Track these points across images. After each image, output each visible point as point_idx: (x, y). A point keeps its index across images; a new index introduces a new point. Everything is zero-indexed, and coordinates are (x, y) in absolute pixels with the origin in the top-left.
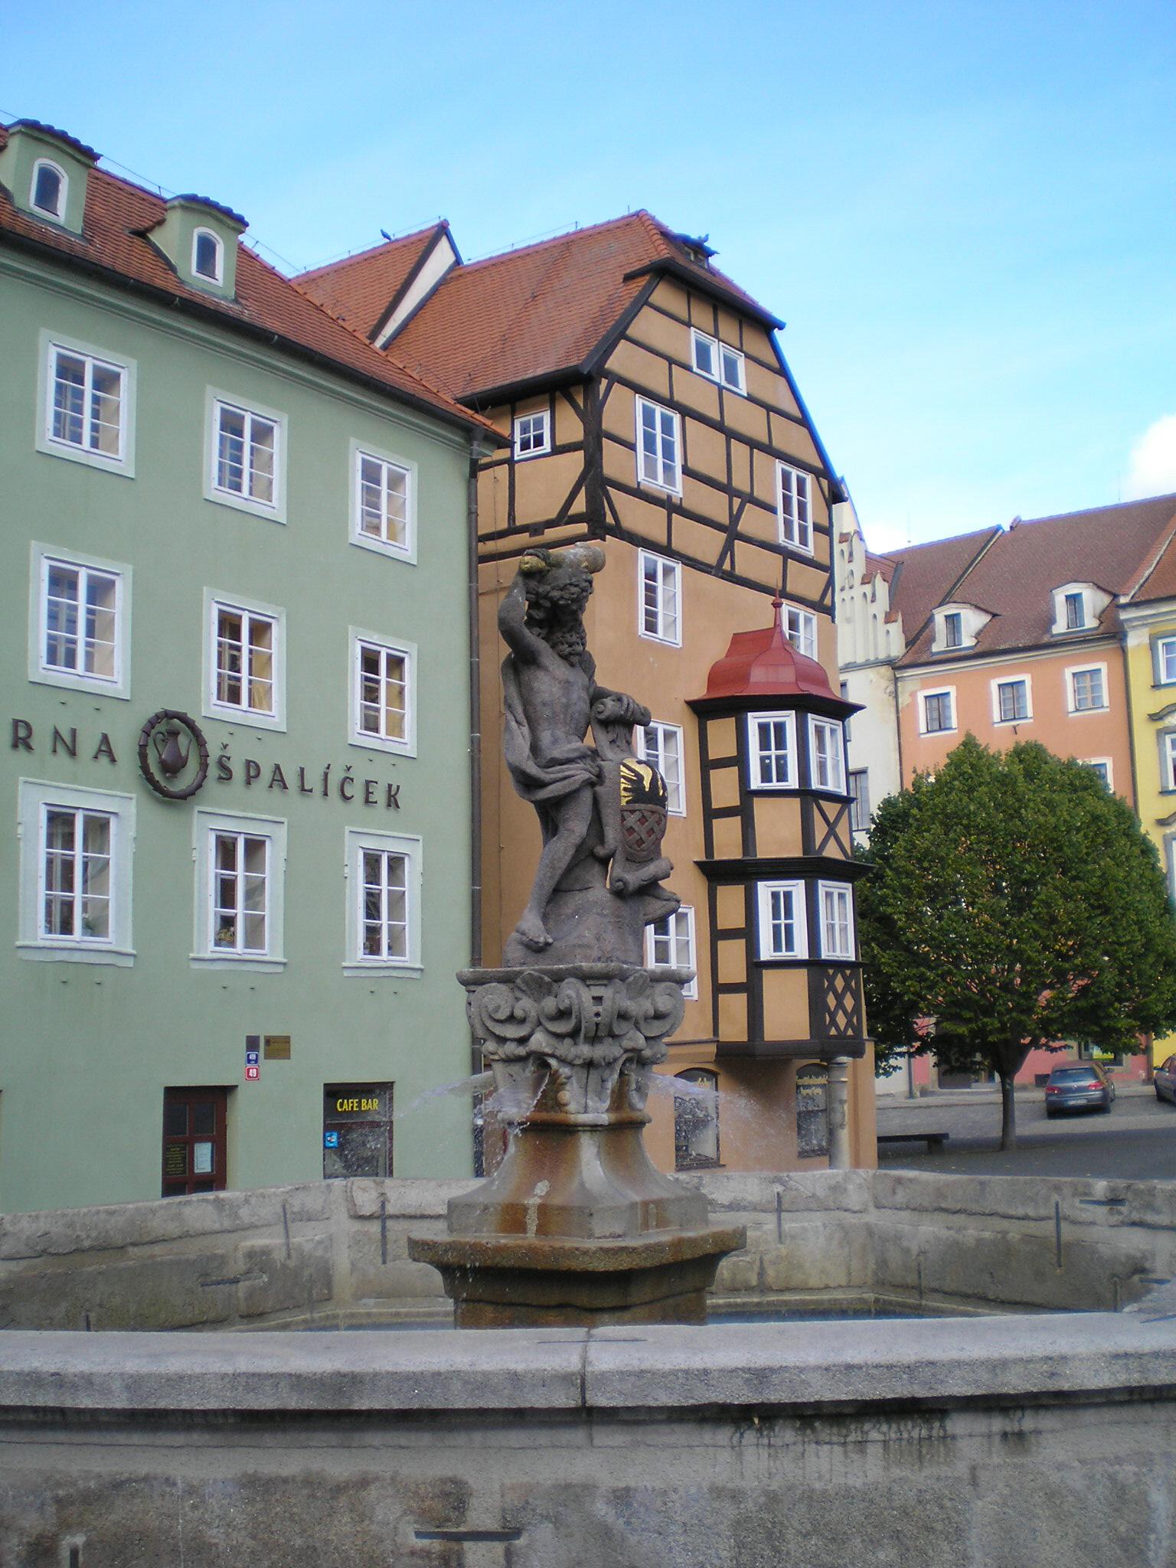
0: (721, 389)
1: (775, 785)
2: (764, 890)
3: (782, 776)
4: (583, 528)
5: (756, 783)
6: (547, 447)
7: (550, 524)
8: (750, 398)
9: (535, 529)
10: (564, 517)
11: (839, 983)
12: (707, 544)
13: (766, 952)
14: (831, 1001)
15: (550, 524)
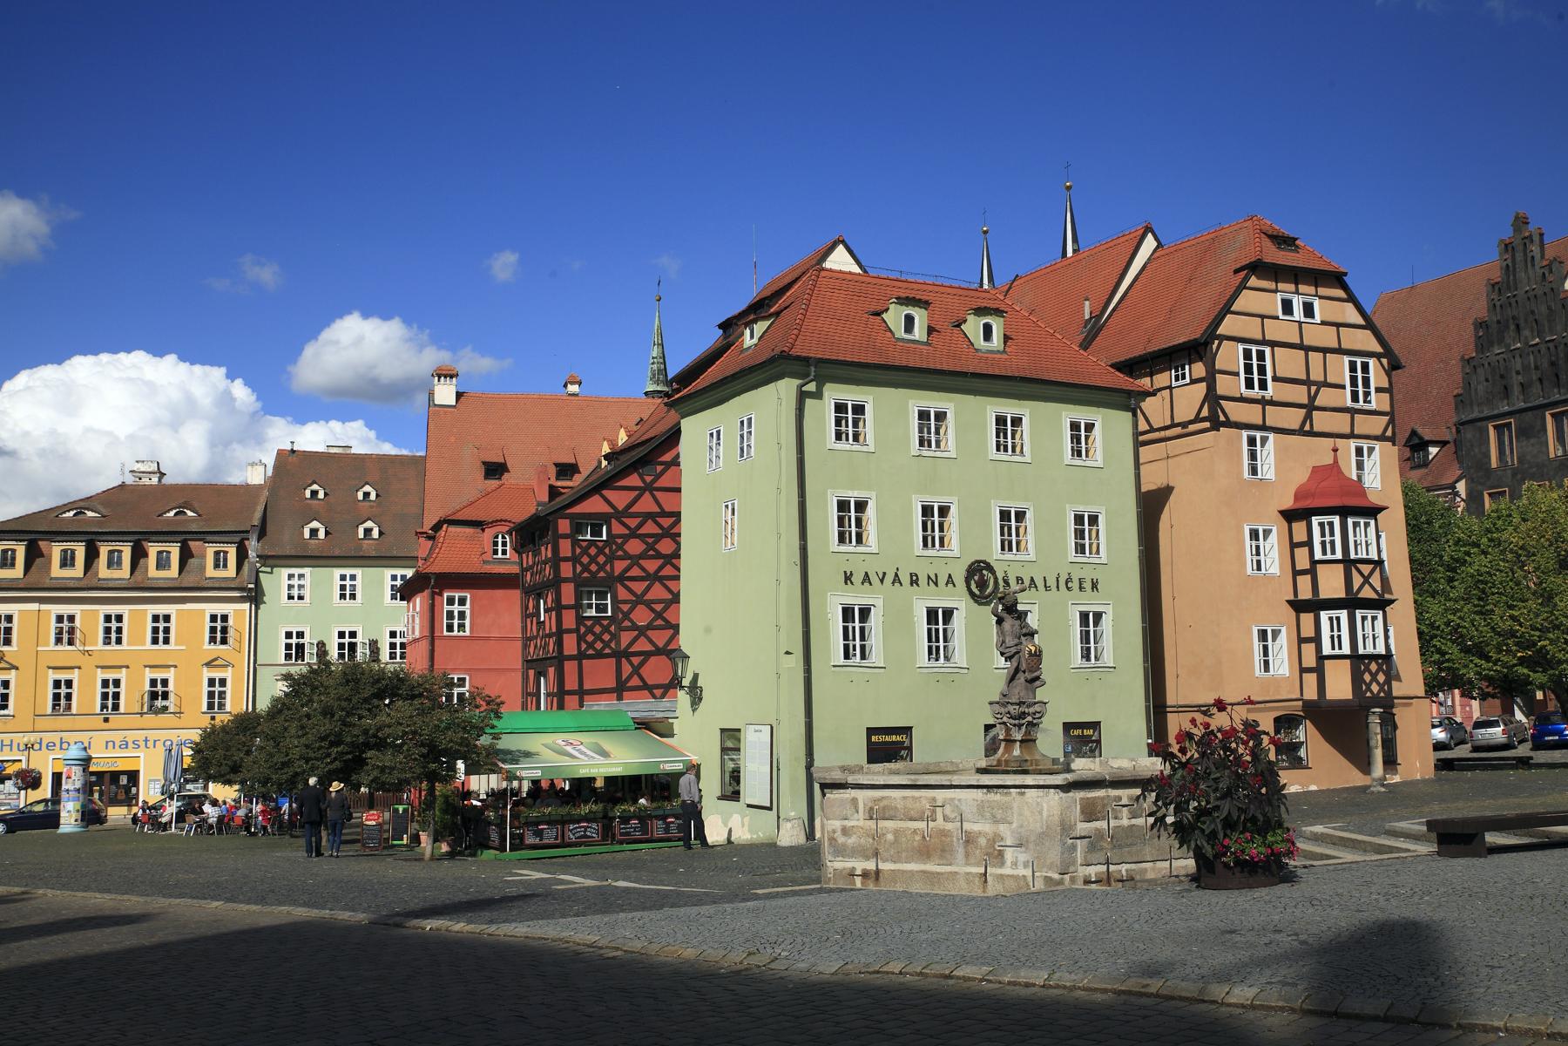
0: (1300, 323)
1: (1329, 557)
2: (1324, 616)
3: (1333, 552)
4: (1207, 424)
5: (1318, 555)
6: (1188, 380)
7: (1191, 422)
8: (1323, 323)
9: (1184, 425)
10: (1197, 419)
11: (1374, 667)
12: (1293, 418)
13: (1327, 650)
14: (1367, 677)
15: (1191, 422)
